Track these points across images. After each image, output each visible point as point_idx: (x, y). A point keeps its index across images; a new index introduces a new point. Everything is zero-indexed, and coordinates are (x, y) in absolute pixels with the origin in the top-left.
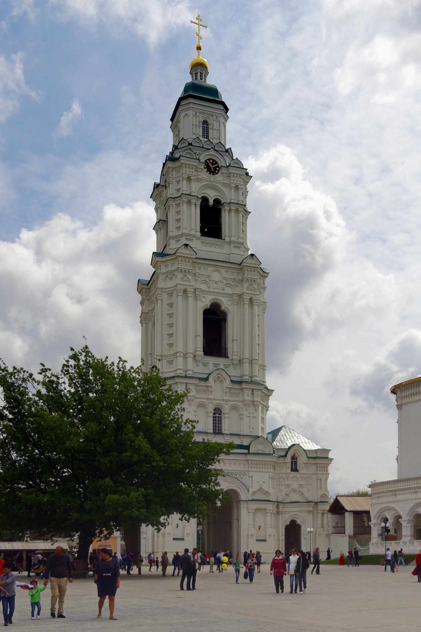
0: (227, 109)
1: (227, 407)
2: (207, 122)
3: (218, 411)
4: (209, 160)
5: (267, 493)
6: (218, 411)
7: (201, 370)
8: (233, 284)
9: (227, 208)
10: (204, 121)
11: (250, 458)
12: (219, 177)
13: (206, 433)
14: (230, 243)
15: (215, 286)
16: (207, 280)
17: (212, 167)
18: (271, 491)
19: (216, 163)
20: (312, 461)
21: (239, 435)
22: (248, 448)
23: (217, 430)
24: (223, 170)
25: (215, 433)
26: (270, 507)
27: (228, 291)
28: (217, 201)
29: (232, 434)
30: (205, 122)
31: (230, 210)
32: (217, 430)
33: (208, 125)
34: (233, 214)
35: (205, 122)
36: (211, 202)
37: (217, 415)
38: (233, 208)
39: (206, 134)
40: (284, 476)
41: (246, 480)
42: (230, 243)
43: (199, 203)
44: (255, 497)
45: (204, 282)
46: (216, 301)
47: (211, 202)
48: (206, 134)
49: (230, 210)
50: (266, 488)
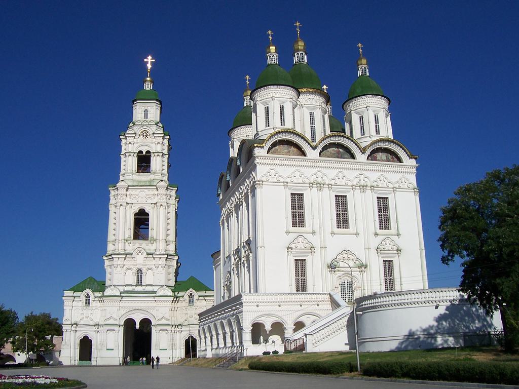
1: (144, 269)
3: (139, 271)
4: (144, 131)
5: (167, 319)
6: (139, 271)
7: (129, 248)
8: (152, 197)
9: (152, 155)
11: (156, 298)
12: (149, 139)
13: (131, 285)
14: (154, 173)
16: (137, 197)
18: (170, 318)
20: (202, 298)
21: (152, 285)
22: (155, 292)
23: (139, 282)
25: (136, 286)
26: (169, 328)
27: (149, 201)
28: (148, 152)
29: (147, 285)
30: (146, 111)
32: (139, 282)
35: (146, 111)
36: (144, 153)
37: (140, 274)
38: (156, 154)
40: (184, 308)
41: (154, 312)
43: (136, 155)
44: (160, 322)
45: (134, 198)
46: (142, 208)
47: (144, 153)
48: (146, 116)
50: (167, 316)
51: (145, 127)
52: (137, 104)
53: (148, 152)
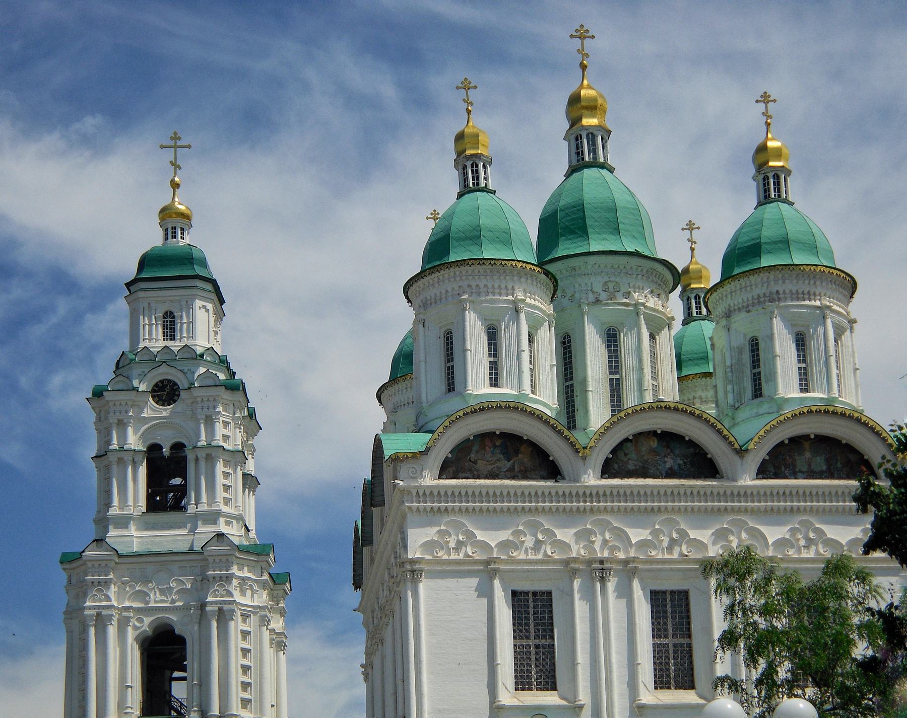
0: (214, 282)
2: (171, 313)
9: (190, 456)
10: (166, 313)
15: (159, 597)
17: (166, 393)
19: (175, 384)
24: (183, 394)
31: (197, 459)
33: (174, 317)
34: (202, 464)
36: (166, 451)
39: (170, 332)
42: (196, 517)
47: (166, 451)
49: (197, 459)
51: (164, 369)
52: (141, 294)
53: (178, 447)
